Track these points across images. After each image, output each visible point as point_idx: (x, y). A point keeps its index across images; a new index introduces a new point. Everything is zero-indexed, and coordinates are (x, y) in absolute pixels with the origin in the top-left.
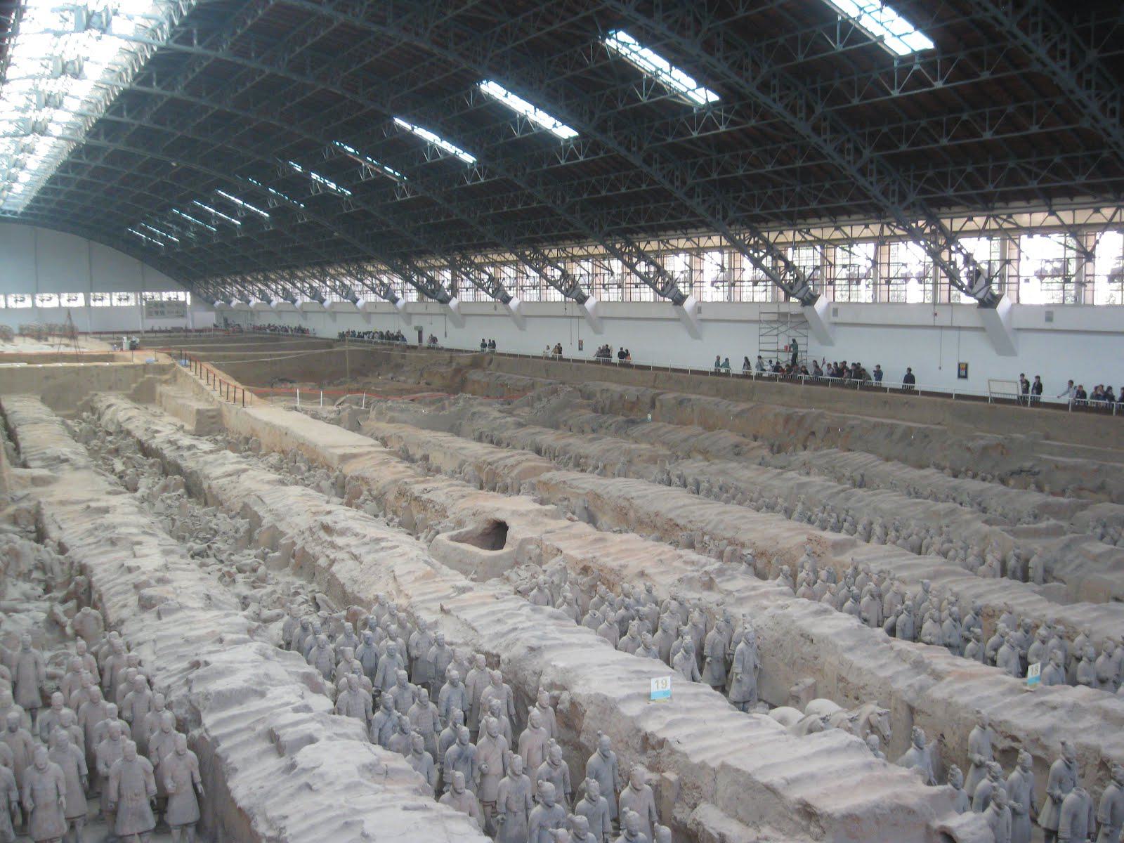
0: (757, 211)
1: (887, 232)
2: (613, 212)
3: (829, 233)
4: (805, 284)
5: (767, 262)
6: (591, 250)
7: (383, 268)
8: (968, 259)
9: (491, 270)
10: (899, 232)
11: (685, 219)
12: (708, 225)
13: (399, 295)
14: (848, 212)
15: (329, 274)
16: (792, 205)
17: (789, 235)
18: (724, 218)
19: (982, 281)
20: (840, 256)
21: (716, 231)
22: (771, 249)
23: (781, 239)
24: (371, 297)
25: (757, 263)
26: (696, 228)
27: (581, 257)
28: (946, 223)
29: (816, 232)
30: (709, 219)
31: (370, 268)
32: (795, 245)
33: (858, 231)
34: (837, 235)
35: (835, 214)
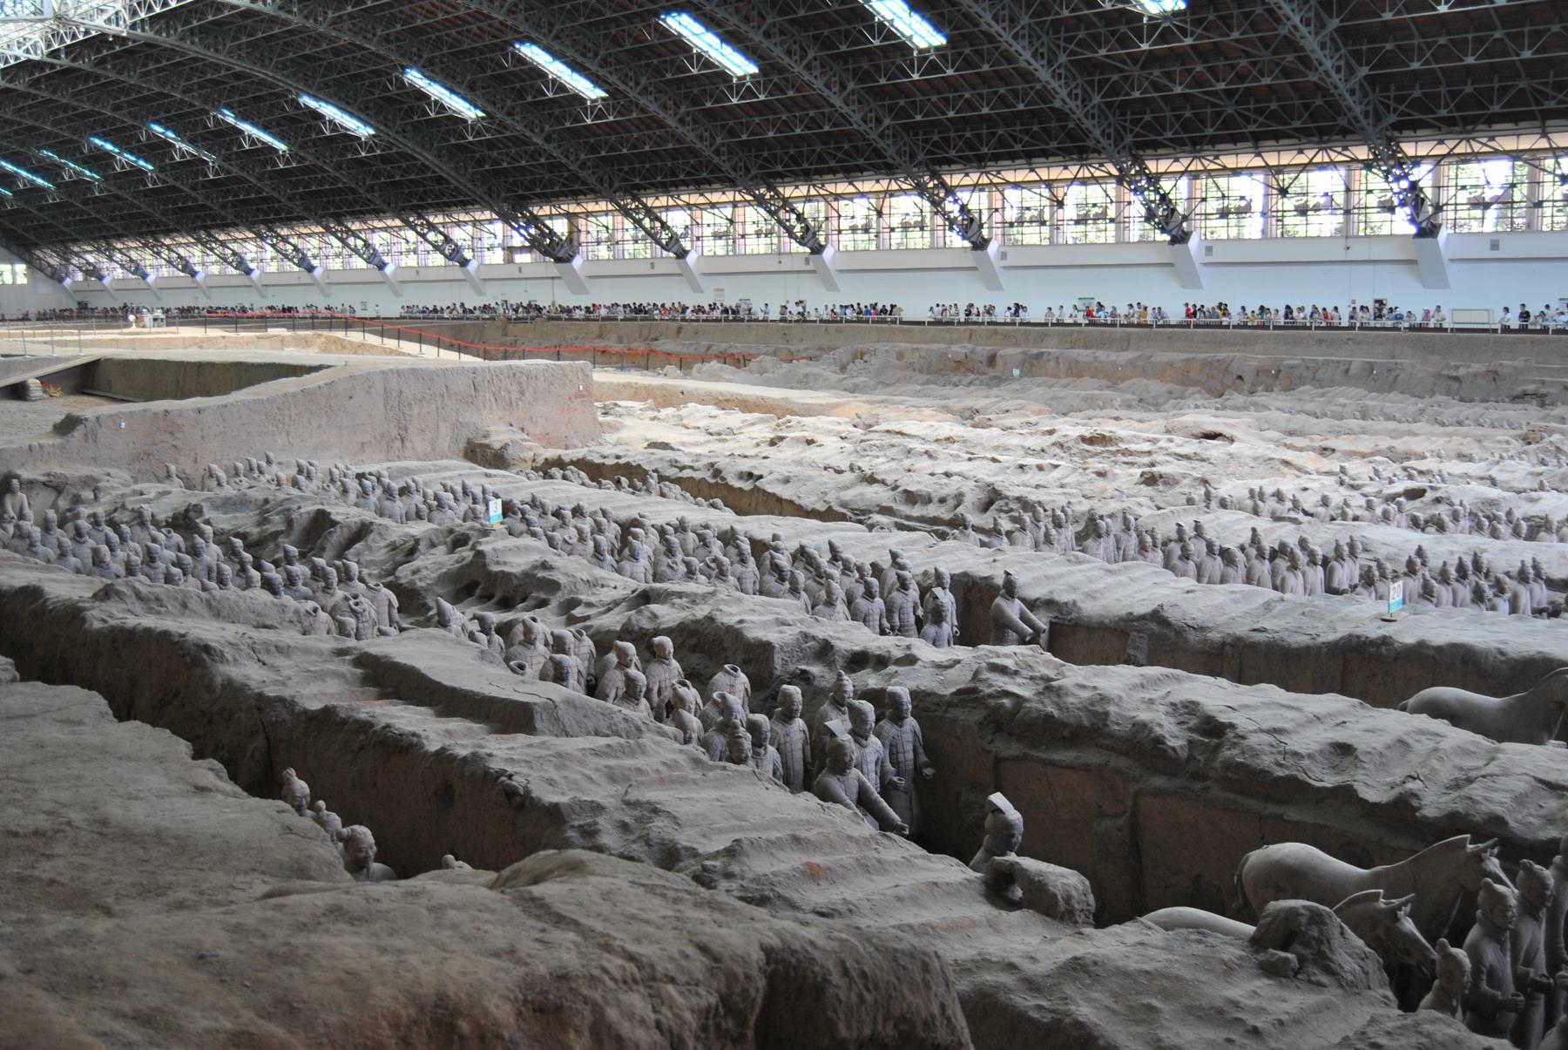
0: (637, 181)
1: (738, 198)
2: (511, 180)
3: (695, 199)
4: (677, 241)
5: (647, 222)
6: (390, 222)
7: (89, 248)
8: (800, 218)
9: (235, 246)
10: (749, 198)
11: (576, 187)
12: (593, 191)
13: (197, 268)
14: (710, 183)
15: (72, 252)
16: (666, 176)
17: (663, 200)
18: (611, 186)
19: (810, 234)
20: (707, 217)
21: (603, 198)
22: (649, 212)
23: (657, 203)
24: (165, 272)
25: (638, 222)
26: (585, 195)
27: (466, 223)
28: (781, 190)
29: (685, 198)
30: (598, 187)
31: (76, 249)
32: (667, 208)
33: (715, 197)
34: (701, 200)
35: (699, 185)
